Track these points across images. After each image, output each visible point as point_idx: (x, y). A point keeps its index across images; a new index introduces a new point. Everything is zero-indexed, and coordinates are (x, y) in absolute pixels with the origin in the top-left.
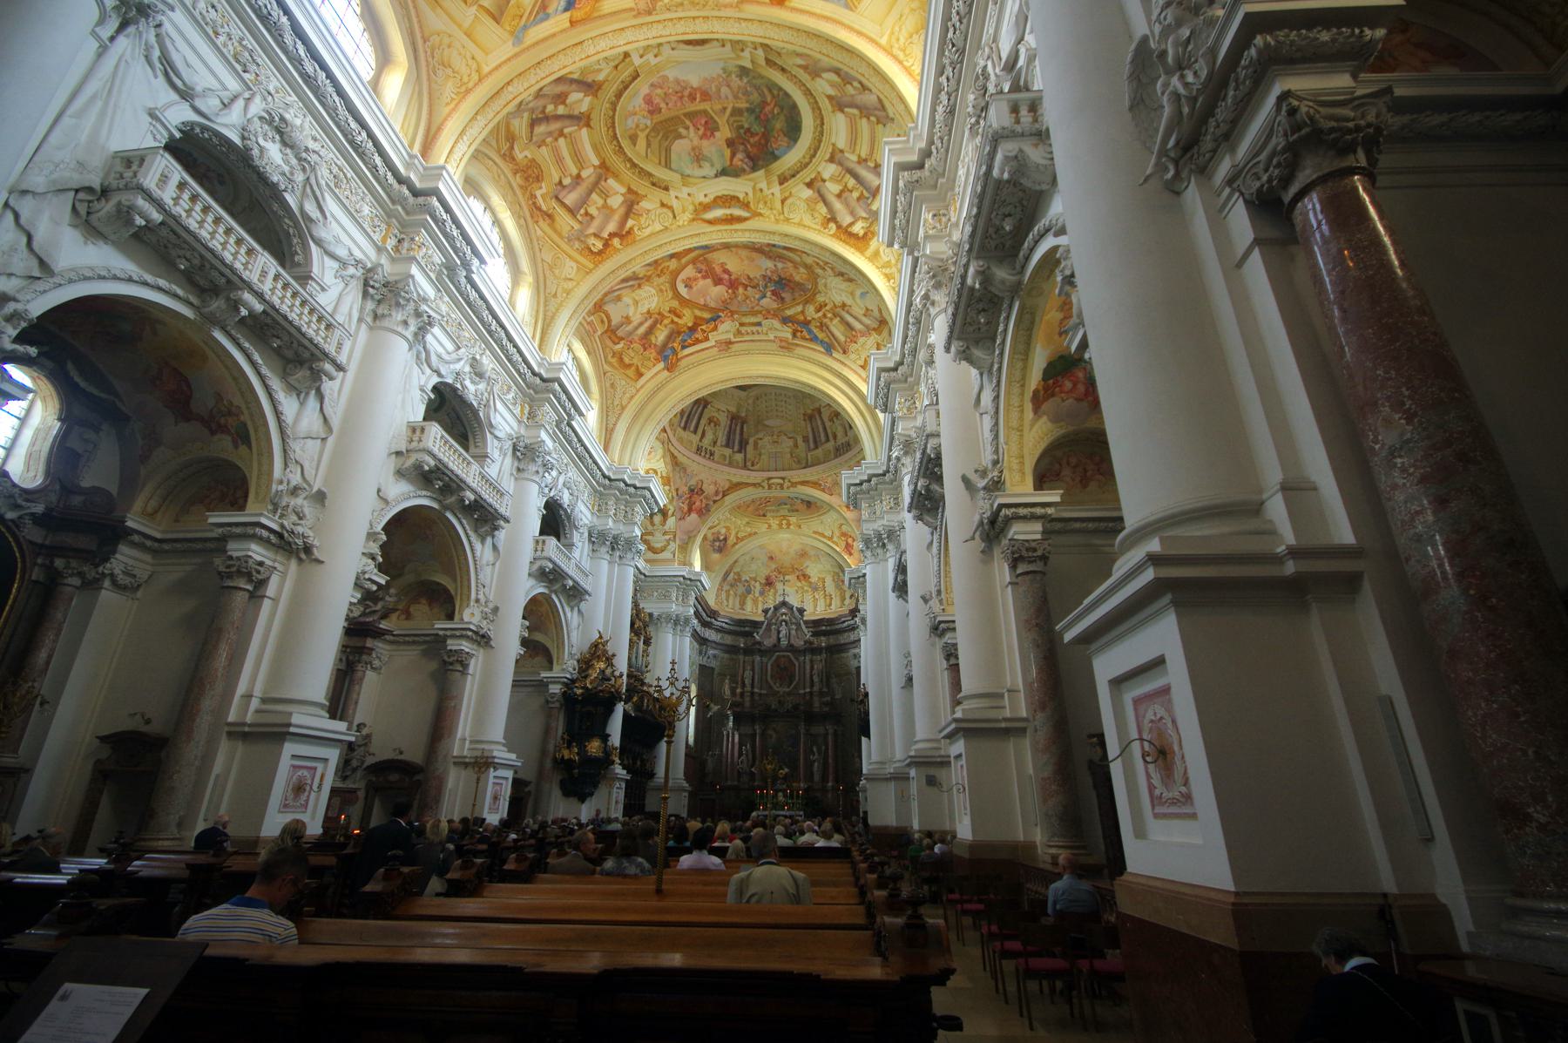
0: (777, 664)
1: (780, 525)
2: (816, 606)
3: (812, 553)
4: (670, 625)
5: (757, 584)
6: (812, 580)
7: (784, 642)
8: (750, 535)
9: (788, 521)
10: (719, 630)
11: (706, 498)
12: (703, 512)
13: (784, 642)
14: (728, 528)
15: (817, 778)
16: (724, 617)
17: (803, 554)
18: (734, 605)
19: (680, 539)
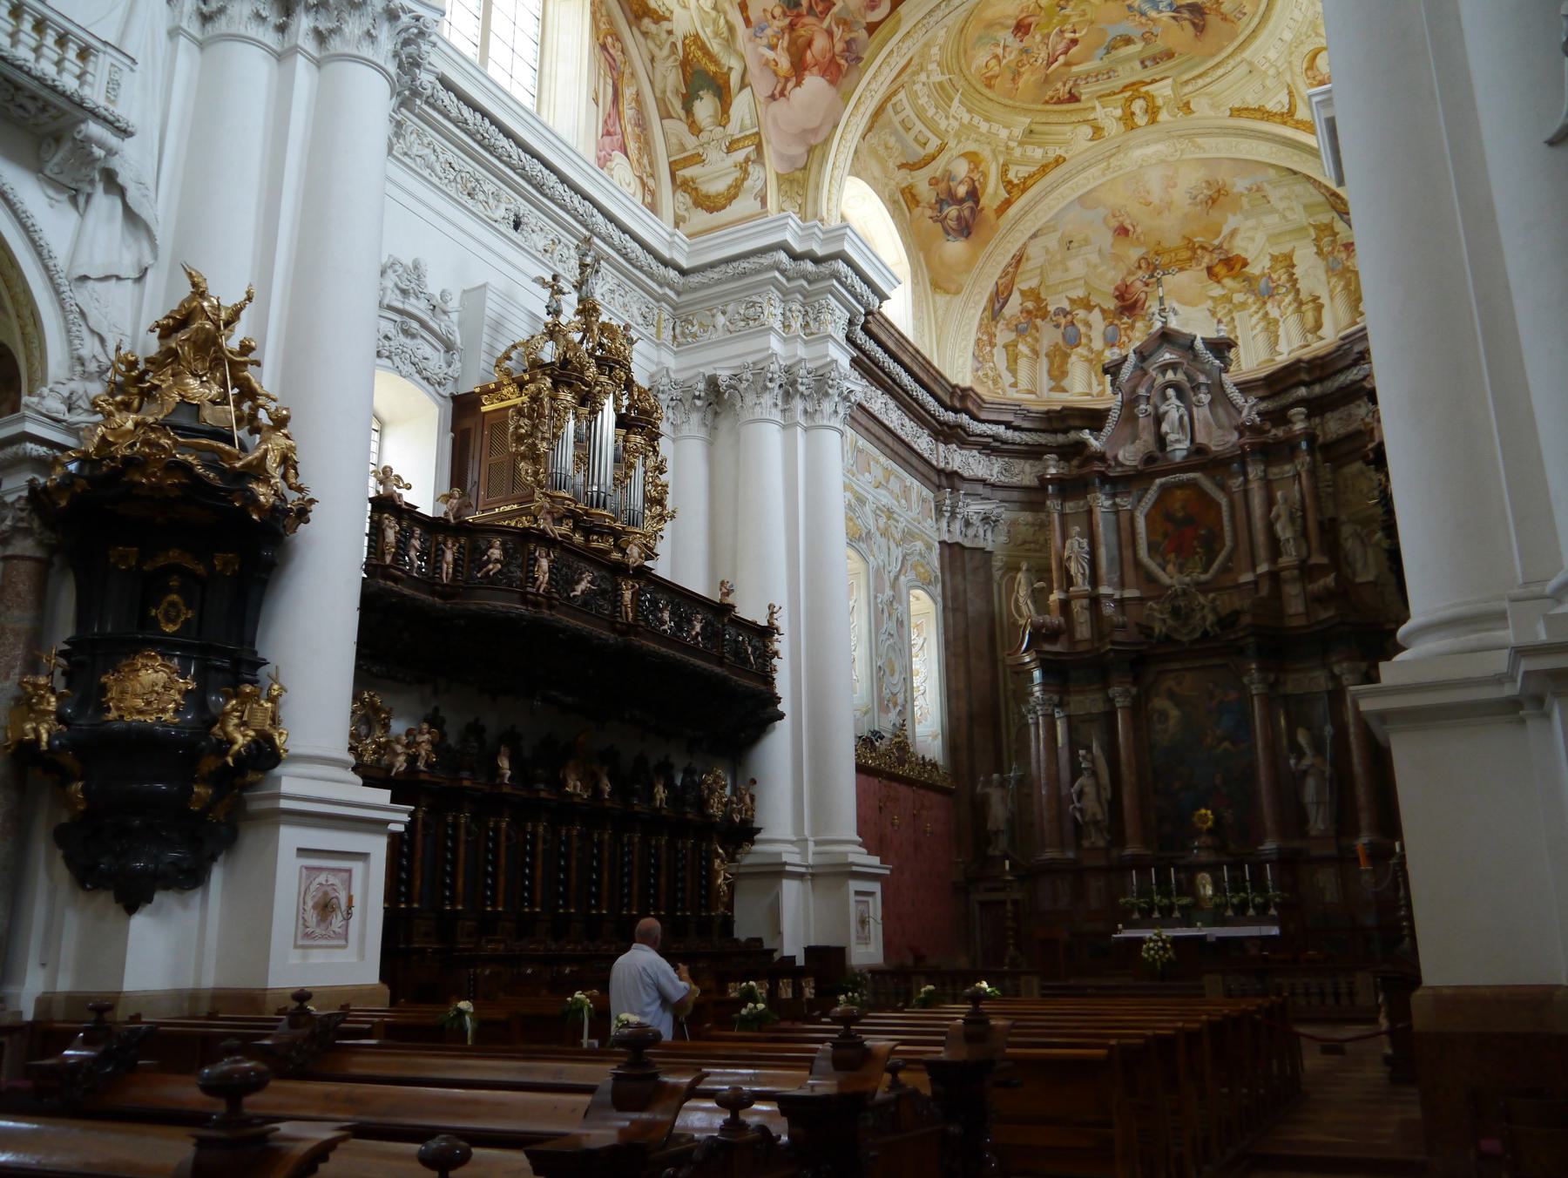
0: (1161, 513)
1: (1128, 119)
2: (1273, 342)
3: (1240, 185)
4: (767, 399)
5: (1096, 317)
6: (1254, 270)
7: (1180, 448)
8: (1044, 169)
9: (1148, 97)
10: (992, 448)
11: (844, 22)
12: (842, 68)
13: (1180, 448)
14: (973, 158)
15: (1318, 822)
16: (1000, 407)
17: (1216, 197)
18: (1033, 383)
19: (781, 157)
